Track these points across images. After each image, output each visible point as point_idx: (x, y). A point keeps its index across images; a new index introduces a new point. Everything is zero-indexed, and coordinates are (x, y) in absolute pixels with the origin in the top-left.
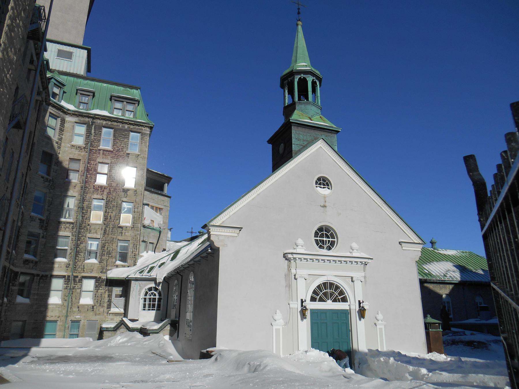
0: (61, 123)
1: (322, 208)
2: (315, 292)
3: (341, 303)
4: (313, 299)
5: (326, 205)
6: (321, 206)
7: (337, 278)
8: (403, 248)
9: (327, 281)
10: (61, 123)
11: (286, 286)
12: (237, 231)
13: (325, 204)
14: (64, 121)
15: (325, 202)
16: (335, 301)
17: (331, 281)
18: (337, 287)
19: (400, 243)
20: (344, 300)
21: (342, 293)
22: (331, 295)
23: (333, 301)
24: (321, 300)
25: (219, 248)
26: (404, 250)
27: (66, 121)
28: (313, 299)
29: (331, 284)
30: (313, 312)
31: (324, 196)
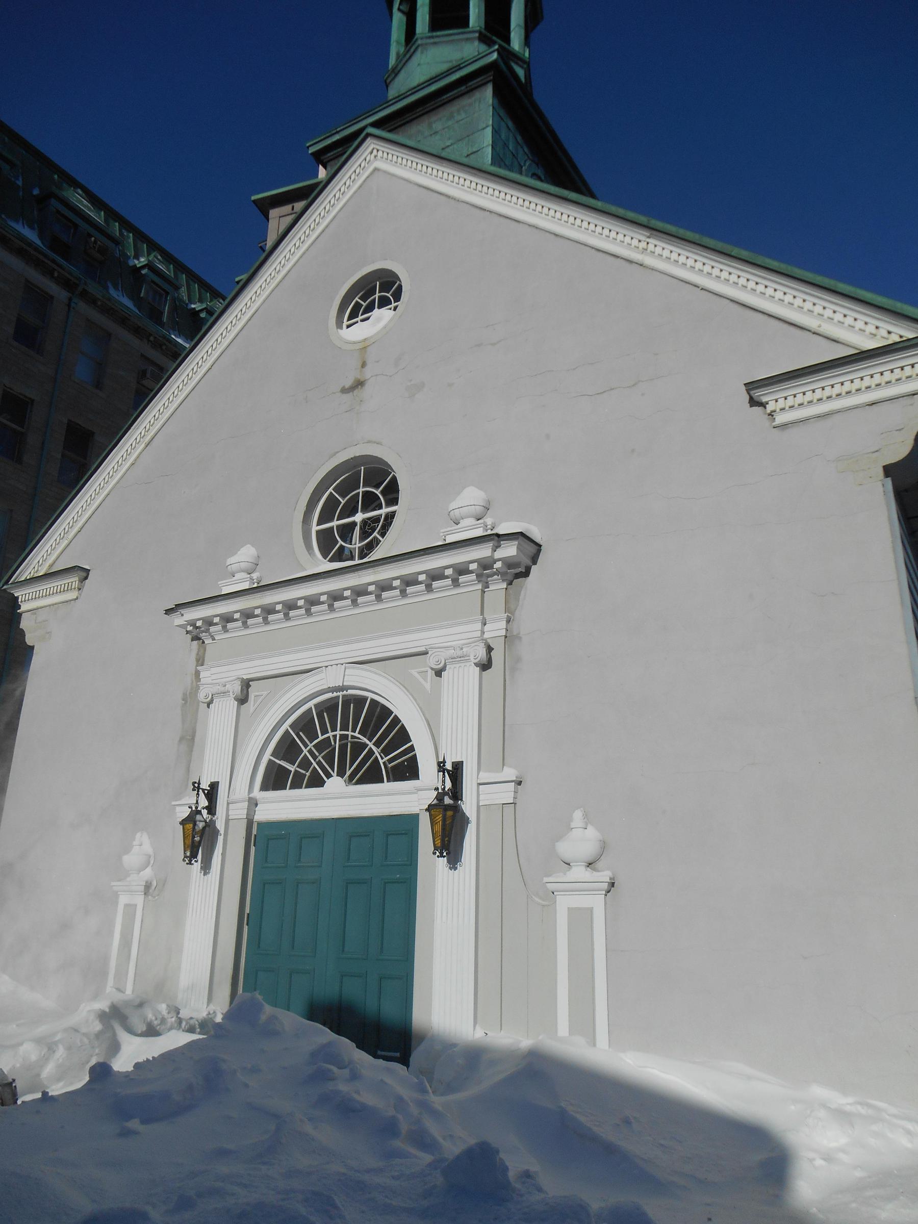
1: (347, 397)
2: (287, 748)
3: (387, 786)
5: (362, 380)
6: (344, 391)
7: (366, 670)
8: (780, 419)
9: (335, 694)
11: (182, 739)
12: (74, 580)
13: (359, 377)
15: (364, 365)
16: (372, 776)
17: (350, 692)
19: (756, 394)
25: (32, 648)
26: (784, 426)
31: (361, 346)
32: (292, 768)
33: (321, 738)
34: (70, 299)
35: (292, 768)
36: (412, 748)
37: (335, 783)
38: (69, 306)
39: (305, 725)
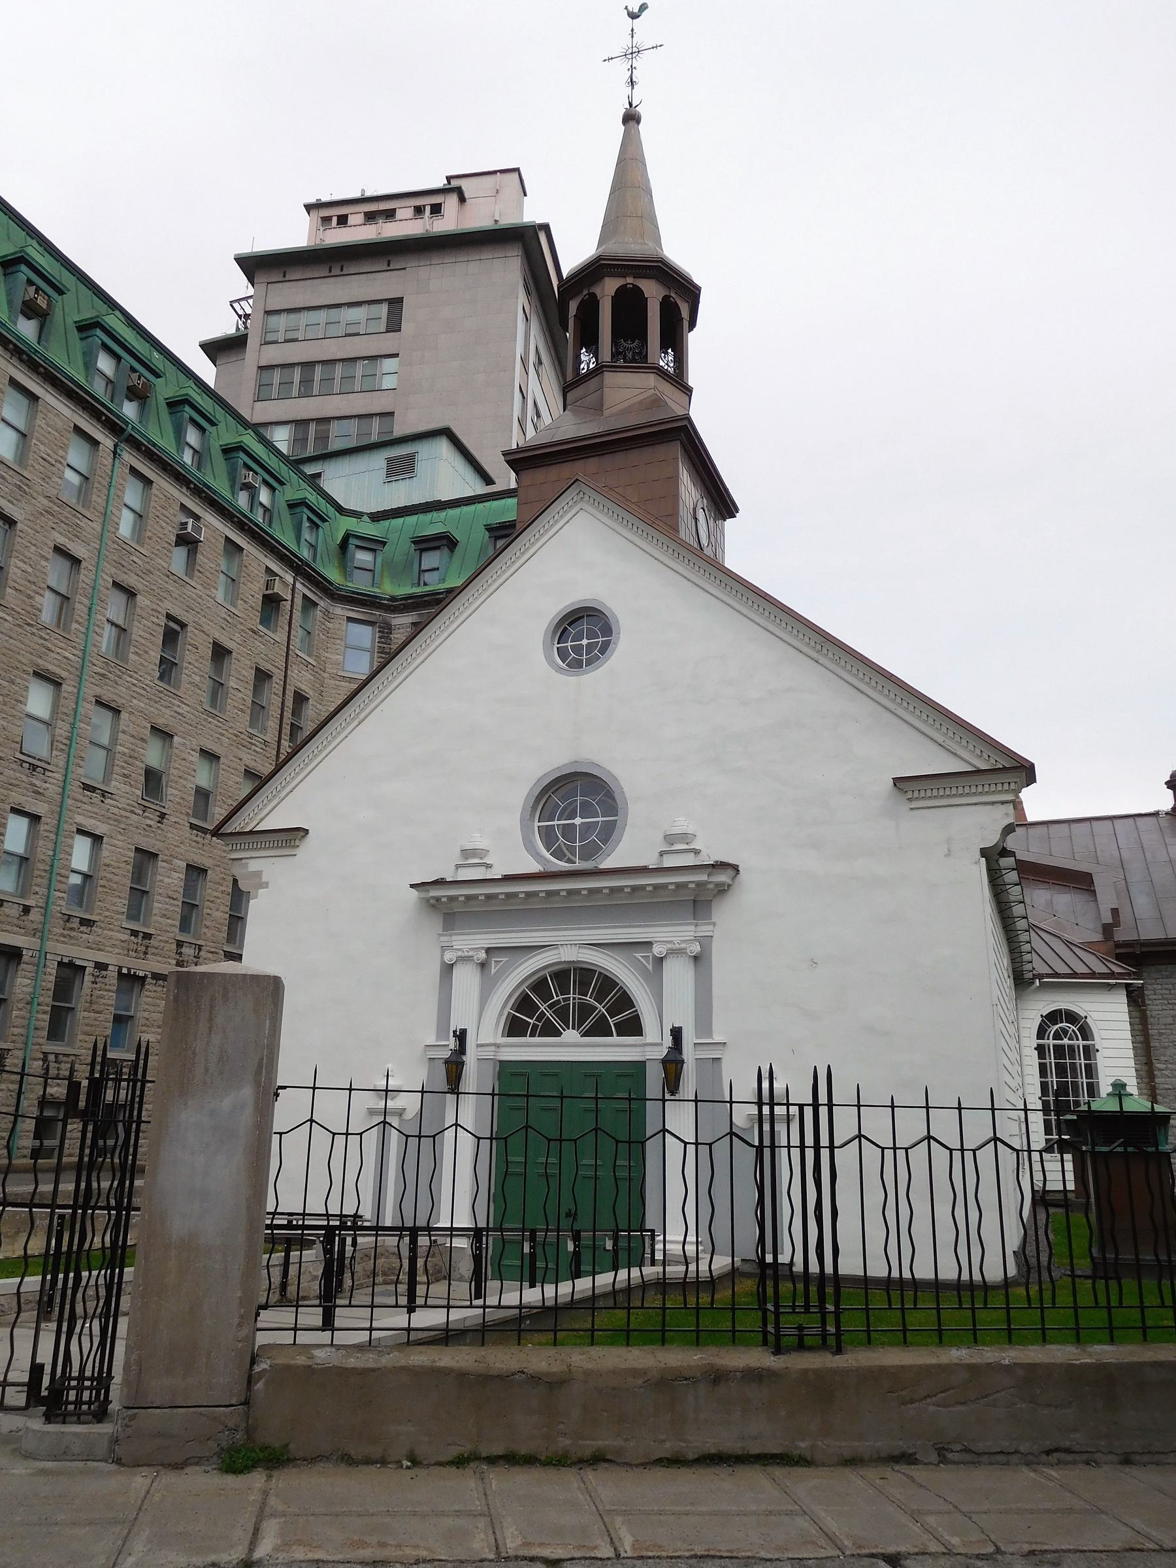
0: (381, 634)
2: (524, 1004)
3: (615, 1039)
4: (515, 1028)
10: (381, 634)
14: (390, 629)
16: (600, 1029)
18: (607, 984)
20: (633, 1027)
21: (625, 1001)
22: (585, 1011)
23: (586, 1034)
24: (550, 1030)
27: (393, 627)
28: (515, 1028)
29: (584, 975)
30: (508, 1071)
32: (531, 1021)
33: (556, 998)
34: (116, 446)
35: (531, 1021)
36: (636, 1011)
37: (571, 1035)
38: (115, 453)
39: (540, 986)
